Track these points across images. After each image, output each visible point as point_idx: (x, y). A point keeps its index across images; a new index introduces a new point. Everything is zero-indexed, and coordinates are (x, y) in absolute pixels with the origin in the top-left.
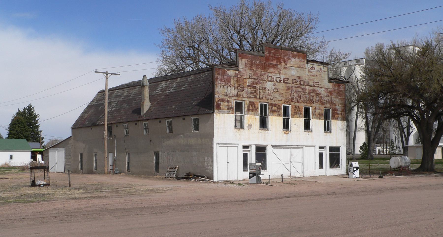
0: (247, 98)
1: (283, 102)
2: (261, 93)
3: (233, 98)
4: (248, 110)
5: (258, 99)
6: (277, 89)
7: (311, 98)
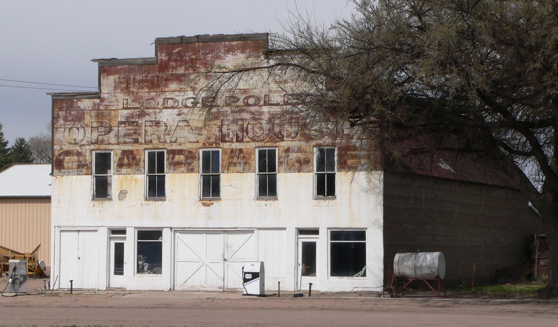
0: (118, 144)
1: (200, 145)
2: (149, 133)
3: (87, 147)
4: (120, 165)
5: (141, 144)
6: (186, 121)
7: (277, 129)
